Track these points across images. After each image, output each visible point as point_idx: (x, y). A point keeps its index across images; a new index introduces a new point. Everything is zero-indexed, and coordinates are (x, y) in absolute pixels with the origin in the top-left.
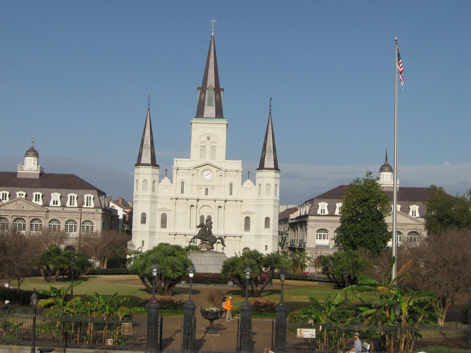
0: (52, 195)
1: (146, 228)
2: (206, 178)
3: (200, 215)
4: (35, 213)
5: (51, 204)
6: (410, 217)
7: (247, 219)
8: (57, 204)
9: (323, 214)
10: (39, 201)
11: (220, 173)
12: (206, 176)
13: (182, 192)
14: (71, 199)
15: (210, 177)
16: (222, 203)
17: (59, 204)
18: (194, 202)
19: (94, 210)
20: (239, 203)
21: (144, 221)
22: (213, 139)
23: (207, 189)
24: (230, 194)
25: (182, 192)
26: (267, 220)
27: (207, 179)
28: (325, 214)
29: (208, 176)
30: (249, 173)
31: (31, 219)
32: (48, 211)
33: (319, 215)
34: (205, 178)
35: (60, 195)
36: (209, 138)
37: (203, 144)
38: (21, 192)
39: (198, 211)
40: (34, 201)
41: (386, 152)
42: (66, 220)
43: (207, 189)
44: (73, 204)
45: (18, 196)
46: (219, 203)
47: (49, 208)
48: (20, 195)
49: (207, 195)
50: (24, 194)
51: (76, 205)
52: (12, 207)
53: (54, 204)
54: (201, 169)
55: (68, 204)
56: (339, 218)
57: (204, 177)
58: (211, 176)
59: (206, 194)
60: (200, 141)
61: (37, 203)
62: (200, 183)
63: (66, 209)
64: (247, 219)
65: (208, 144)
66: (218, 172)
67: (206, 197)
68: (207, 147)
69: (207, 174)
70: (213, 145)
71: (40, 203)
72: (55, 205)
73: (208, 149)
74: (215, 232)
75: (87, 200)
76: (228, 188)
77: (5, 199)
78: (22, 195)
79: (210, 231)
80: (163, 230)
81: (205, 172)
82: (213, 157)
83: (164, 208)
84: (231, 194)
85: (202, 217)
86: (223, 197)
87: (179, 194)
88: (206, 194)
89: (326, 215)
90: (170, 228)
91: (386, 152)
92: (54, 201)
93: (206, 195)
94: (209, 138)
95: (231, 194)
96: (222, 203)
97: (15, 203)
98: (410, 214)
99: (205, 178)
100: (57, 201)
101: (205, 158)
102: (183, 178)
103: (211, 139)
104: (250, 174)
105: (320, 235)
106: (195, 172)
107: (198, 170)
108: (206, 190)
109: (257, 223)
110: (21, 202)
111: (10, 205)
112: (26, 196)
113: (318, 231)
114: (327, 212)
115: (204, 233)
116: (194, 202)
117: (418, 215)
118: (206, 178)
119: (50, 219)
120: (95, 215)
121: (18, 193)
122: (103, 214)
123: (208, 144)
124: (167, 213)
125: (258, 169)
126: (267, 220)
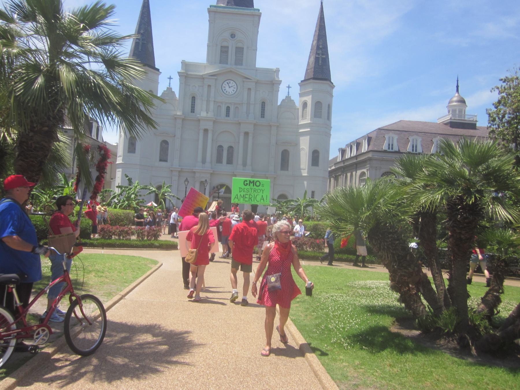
9: (390, 150)
12: (227, 88)
15: (233, 90)
23: (228, 109)
24: (262, 117)
28: (393, 151)
30: (289, 87)
36: (233, 36)
37: (225, 44)
41: (458, 81)
43: (228, 109)
49: (229, 116)
58: (235, 90)
59: (228, 115)
65: (232, 45)
69: (230, 85)
70: (240, 45)
80: (164, 164)
81: (226, 83)
82: (239, 61)
88: (228, 115)
91: (458, 81)
93: (226, 116)
94: (233, 36)
101: (227, 63)
103: (236, 37)
107: (216, 79)
108: (227, 109)
125: (302, 81)
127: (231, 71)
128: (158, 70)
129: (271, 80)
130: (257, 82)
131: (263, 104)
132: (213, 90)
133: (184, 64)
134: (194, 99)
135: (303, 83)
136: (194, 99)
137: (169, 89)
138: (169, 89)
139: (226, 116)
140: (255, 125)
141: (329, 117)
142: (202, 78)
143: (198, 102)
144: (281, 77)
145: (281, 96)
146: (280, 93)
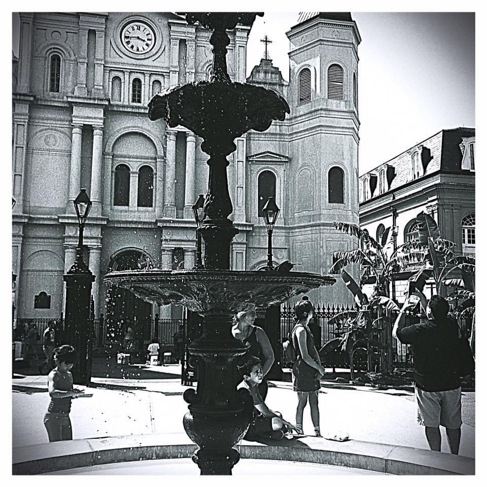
2: (135, 48)
3: (119, 161)
15: (147, 45)
23: (137, 82)
27: (138, 50)
30: (266, 41)
34: (132, 47)
39: (109, 149)
43: (137, 82)
57: (128, 43)
58: (151, 43)
66: (173, 28)
93: (134, 101)
99: (132, 47)
104: (269, 45)
108: (134, 86)
118: (135, 48)
139: (134, 101)
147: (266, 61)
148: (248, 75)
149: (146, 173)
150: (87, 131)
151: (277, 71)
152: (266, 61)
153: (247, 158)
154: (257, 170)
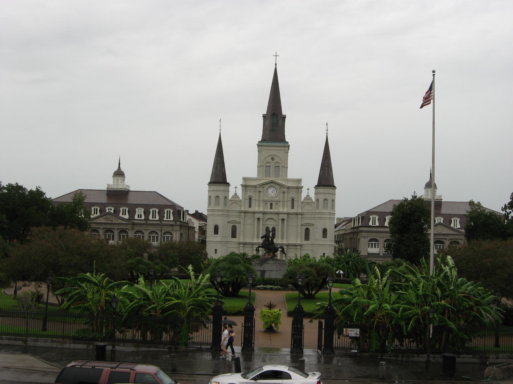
0: (137, 210)
1: (218, 238)
3: (267, 226)
4: (122, 225)
5: (136, 217)
6: (452, 229)
7: (307, 230)
8: (141, 217)
10: (125, 214)
11: (283, 190)
13: (250, 206)
14: (153, 213)
16: (285, 217)
17: (143, 217)
18: (260, 216)
19: (173, 223)
20: (300, 216)
21: (216, 231)
22: (277, 159)
23: (271, 204)
25: (250, 206)
26: (325, 231)
29: (272, 192)
31: (119, 230)
32: (134, 224)
33: (371, 227)
35: (143, 210)
36: (273, 159)
37: (268, 165)
38: (110, 208)
40: (121, 215)
42: (149, 231)
43: (271, 204)
44: (155, 218)
45: (107, 211)
46: (281, 216)
47: (135, 222)
48: (109, 209)
50: (113, 209)
51: (157, 218)
52: (102, 220)
53: (138, 217)
54: (266, 187)
55: (151, 218)
56: (388, 230)
59: (271, 208)
60: (265, 162)
61: (124, 216)
62: (266, 198)
63: (148, 222)
64: (307, 231)
65: (272, 165)
67: (271, 210)
68: (271, 167)
71: (127, 217)
72: (140, 218)
73: (272, 169)
74: (277, 241)
75: (167, 214)
76: (290, 203)
77: (97, 214)
78: (111, 210)
79: (272, 241)
82: (277, 175)
83: (234, 221)
84: (293, 208)
85: (267, 229)
86: (285, 210)
87: (248, 209)
88: (271, 208)
89: (377, 227)
90: (240, 238)
92: (138, 215)
94: (273, 159)
95: (293, 208)
96: (285, 217)
97: (105, 217)
98: (452, 225)
100: (141, 215)
102: (250, 194)
105: (372, 244)
106: (261, 189)
109: (316, 234)
110: (110, 216)
111: (100, 219)
112: (114, 211)
113: (371, 240)
114: (377, 224)
115: (266, 243)
116: (260, 216)
117: (459, 226)
119: (135, 231)
120: (174, 227)
121: (107, 209)
122: (181, 226)
123: (272, 165)
124: (237, 225)
126: (325, 231)
127: (272, 182)
128: (229, 183)
129: (297, 187)
130: (289, 188)
131: (293, 200)
132: (262, 194)
133: (245, 179)
134: (250, 199)
135: (317, 187)
136: (250, 199)
137: (236, 194)
138: (236, 194)
140: (288, 214)
141: (333, 207)
142: (255, 187)
143: (253, 202)
144: (303, 184)
145: (304, 195)
146: (302, 193)
147: (308, 196)
148: (302, 200)
149: (274, 229)
150: (259, 219)
151: (311, 199)
152: (308, 196)
153: (302, 225)
154: (304, 228)
